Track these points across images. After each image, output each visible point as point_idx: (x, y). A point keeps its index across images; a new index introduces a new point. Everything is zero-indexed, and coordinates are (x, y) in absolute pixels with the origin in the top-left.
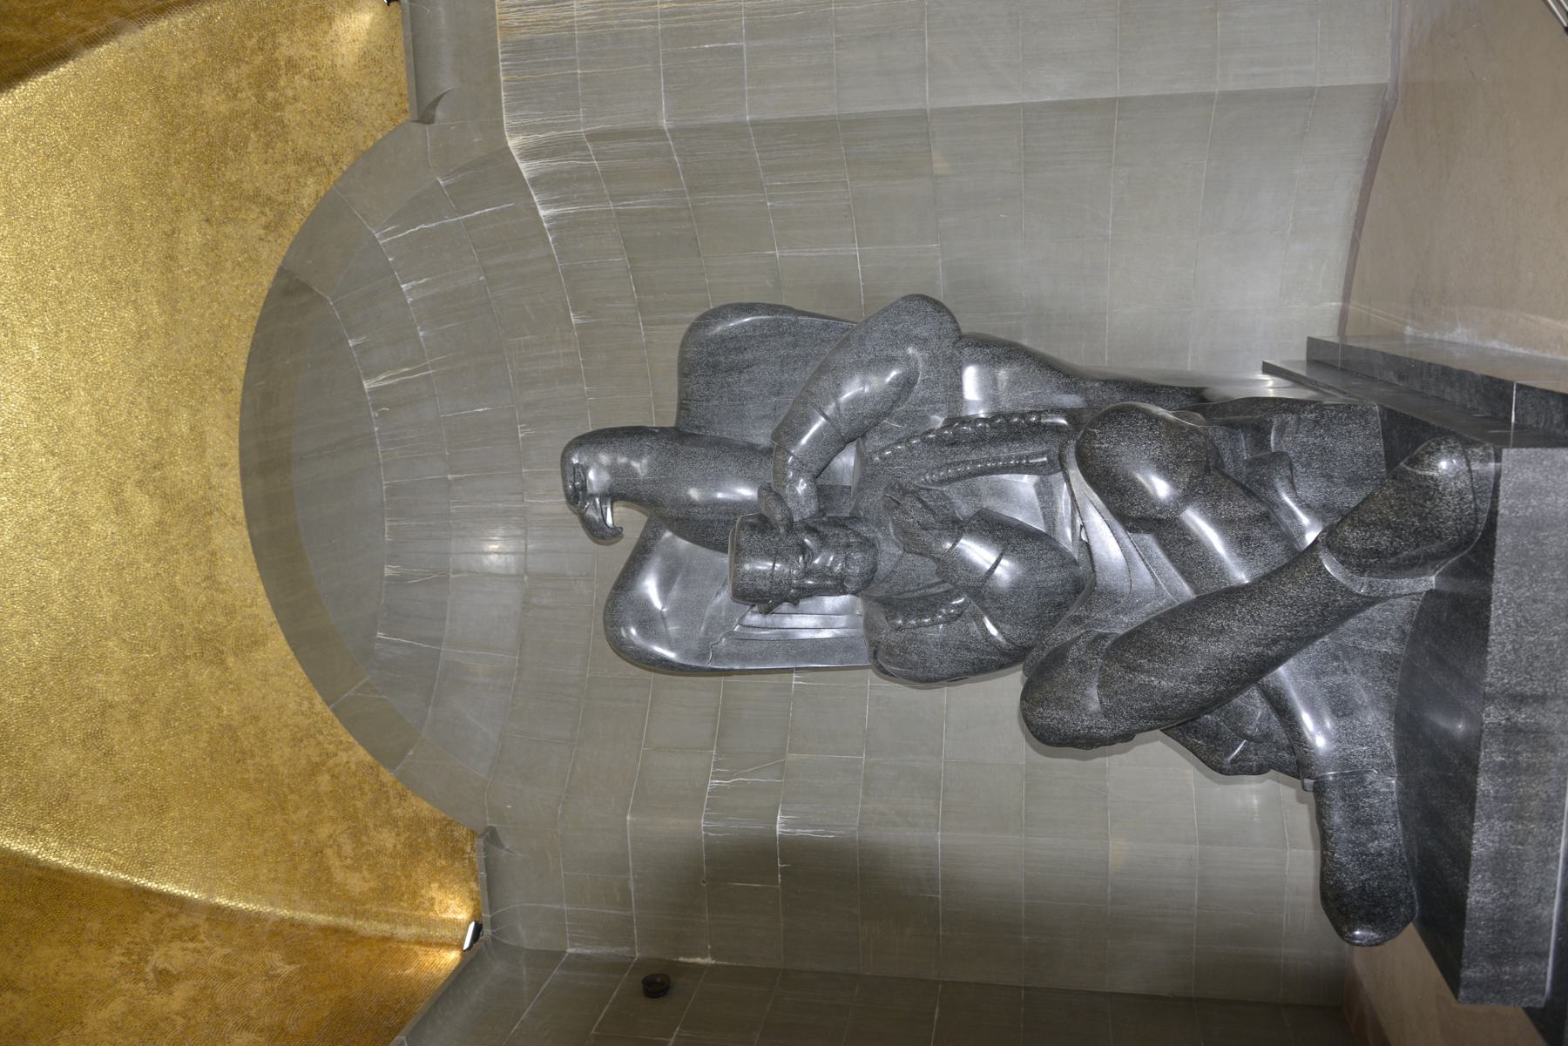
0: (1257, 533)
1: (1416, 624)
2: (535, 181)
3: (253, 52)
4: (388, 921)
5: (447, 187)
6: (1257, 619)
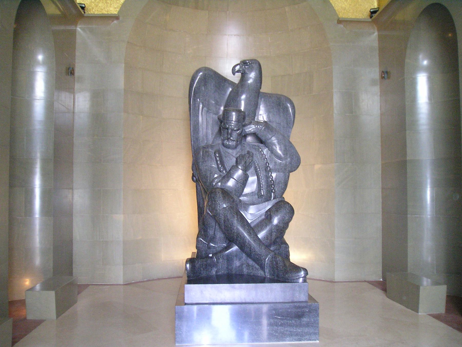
1: (254, 275)
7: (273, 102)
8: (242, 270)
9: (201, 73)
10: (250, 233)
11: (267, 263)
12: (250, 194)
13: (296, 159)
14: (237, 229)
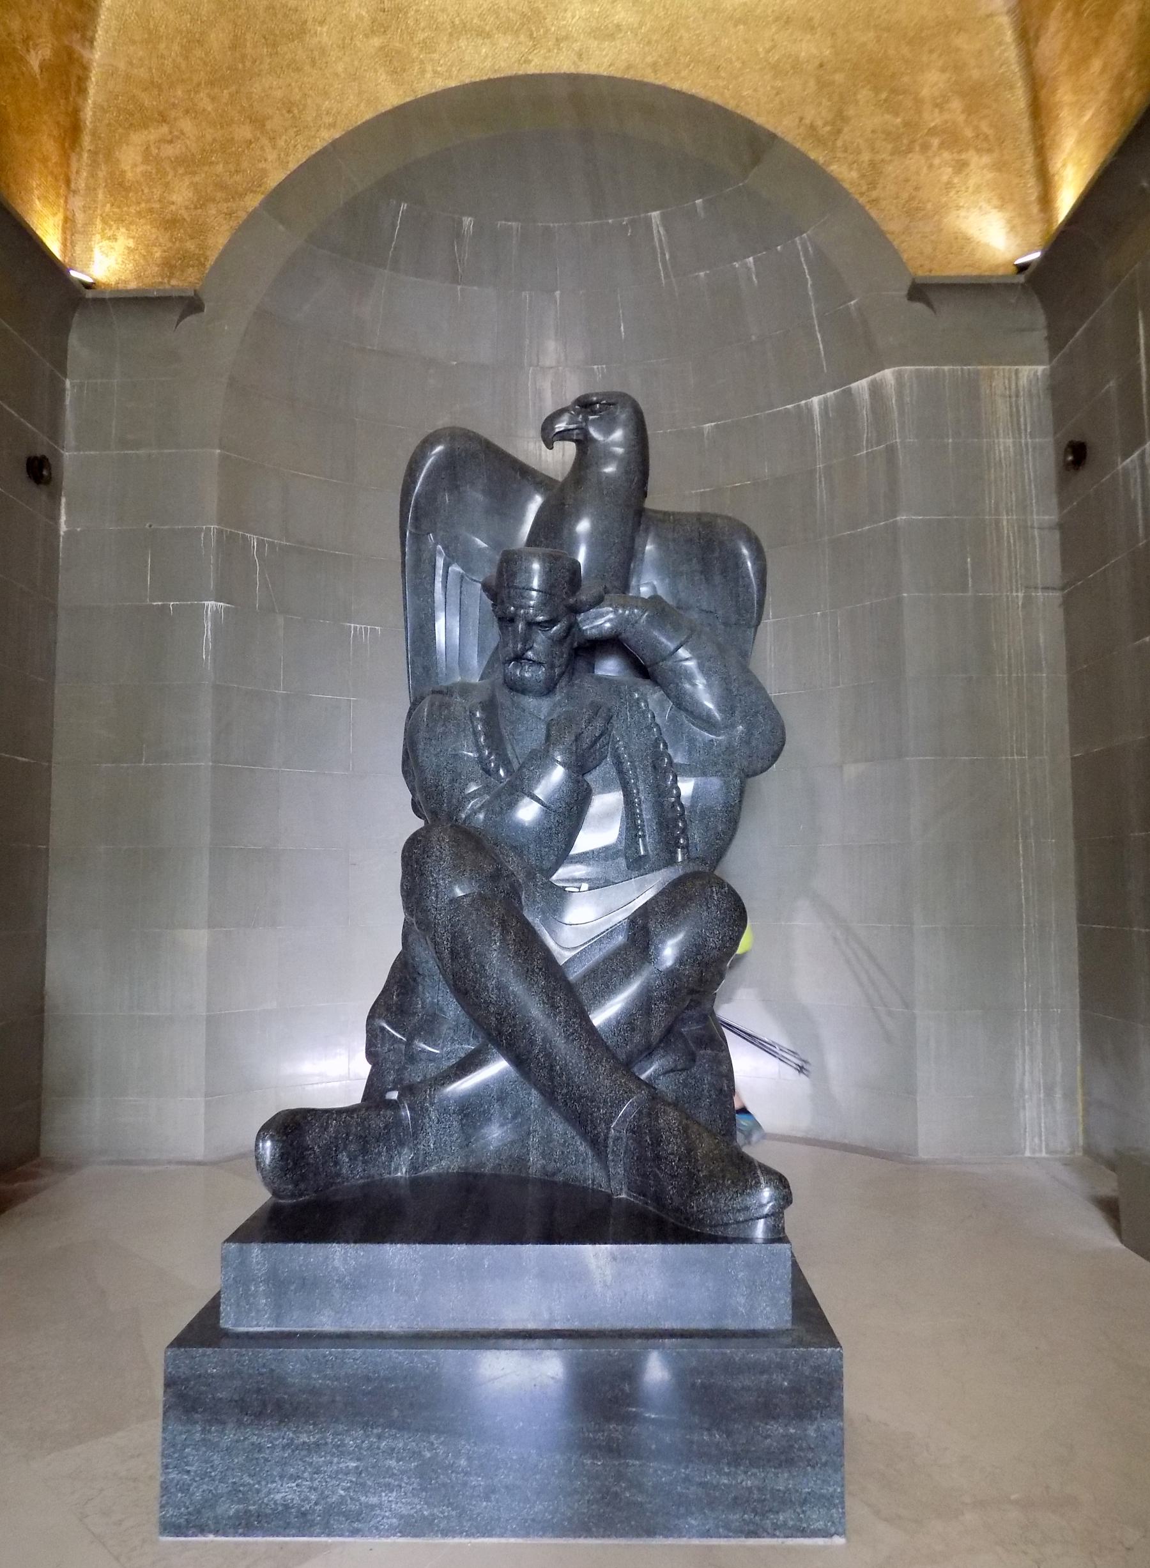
0: (637, 1038)
1: (566, 1184)
2: (848, 392)
3: (976, 128)
4: (88, 188)
5: (848, 308)
6: (571, 1038)
7: (690, 541)
8: (522, 1161)
9: (439, 449)
10: (554, 1006)
11: (617, 1139)
12: (599, 853)
13: (769, 727)
14: (500, 987)
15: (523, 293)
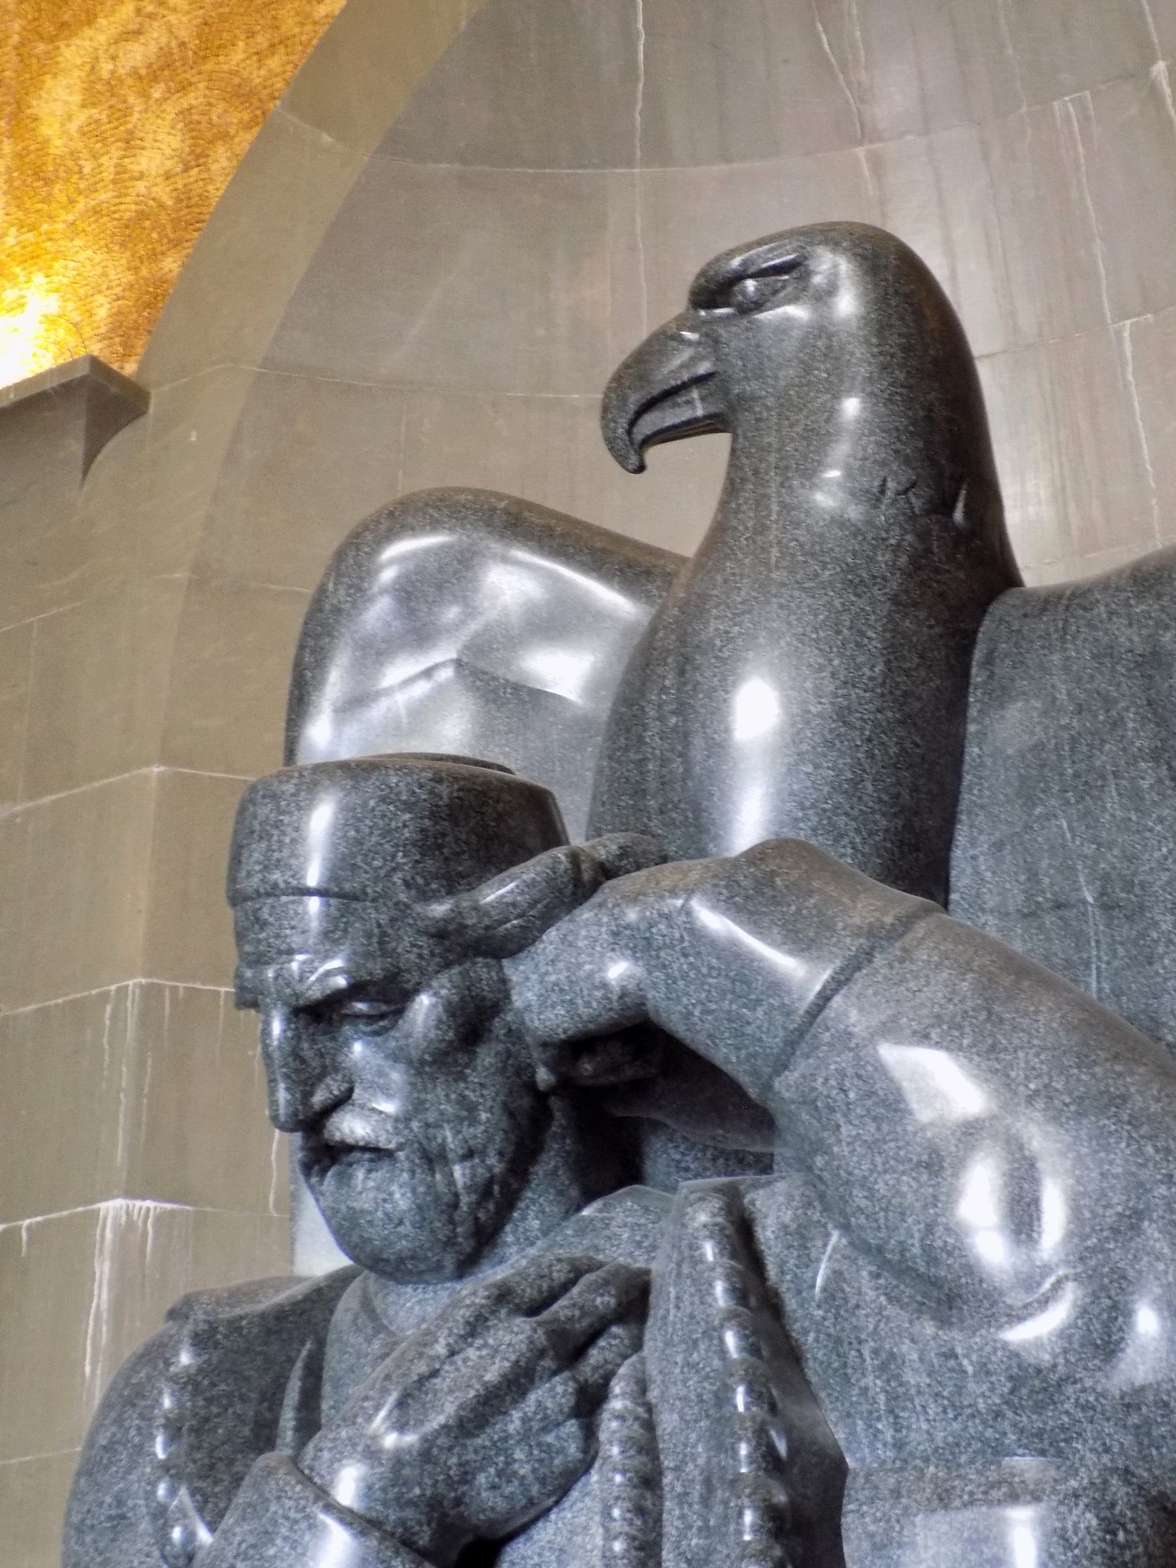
15: (1056, 105)
